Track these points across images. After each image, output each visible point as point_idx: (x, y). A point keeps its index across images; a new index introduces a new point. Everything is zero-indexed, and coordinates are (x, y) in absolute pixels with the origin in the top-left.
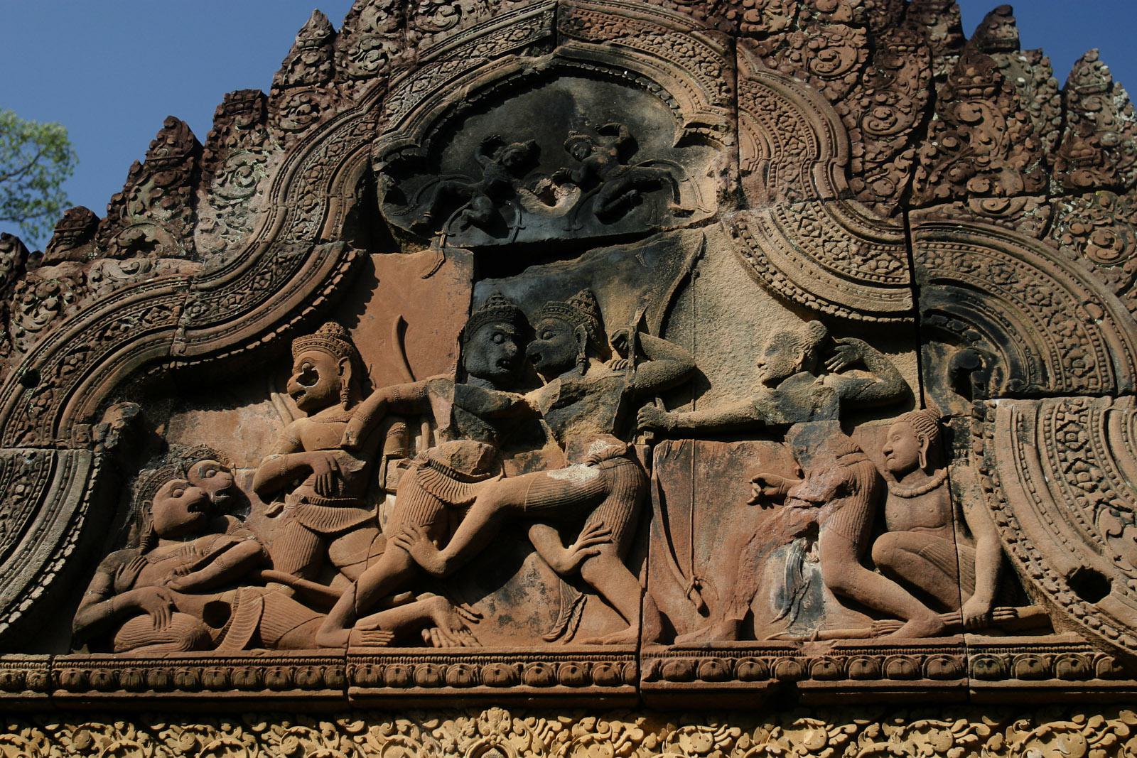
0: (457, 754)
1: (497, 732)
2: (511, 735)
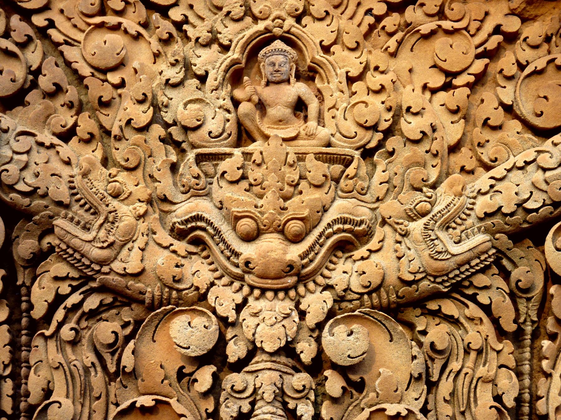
0: (215, 47)
1: (283, 14)
2: (306, 20)
